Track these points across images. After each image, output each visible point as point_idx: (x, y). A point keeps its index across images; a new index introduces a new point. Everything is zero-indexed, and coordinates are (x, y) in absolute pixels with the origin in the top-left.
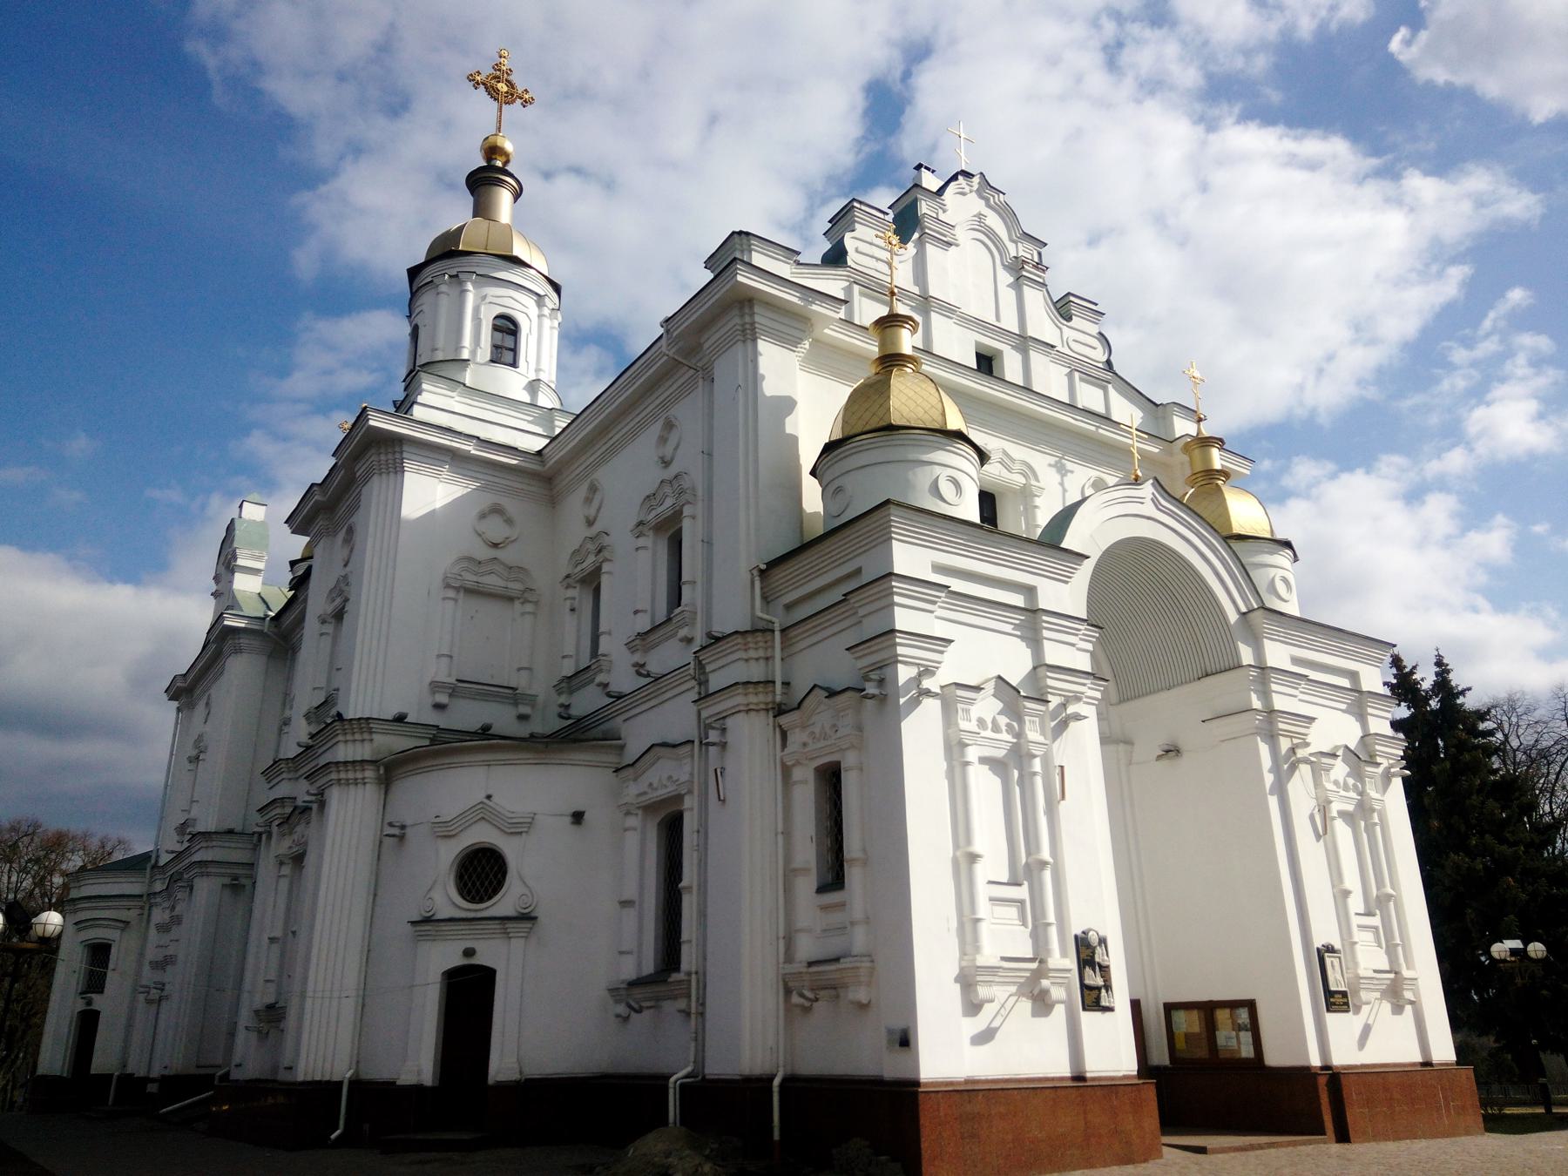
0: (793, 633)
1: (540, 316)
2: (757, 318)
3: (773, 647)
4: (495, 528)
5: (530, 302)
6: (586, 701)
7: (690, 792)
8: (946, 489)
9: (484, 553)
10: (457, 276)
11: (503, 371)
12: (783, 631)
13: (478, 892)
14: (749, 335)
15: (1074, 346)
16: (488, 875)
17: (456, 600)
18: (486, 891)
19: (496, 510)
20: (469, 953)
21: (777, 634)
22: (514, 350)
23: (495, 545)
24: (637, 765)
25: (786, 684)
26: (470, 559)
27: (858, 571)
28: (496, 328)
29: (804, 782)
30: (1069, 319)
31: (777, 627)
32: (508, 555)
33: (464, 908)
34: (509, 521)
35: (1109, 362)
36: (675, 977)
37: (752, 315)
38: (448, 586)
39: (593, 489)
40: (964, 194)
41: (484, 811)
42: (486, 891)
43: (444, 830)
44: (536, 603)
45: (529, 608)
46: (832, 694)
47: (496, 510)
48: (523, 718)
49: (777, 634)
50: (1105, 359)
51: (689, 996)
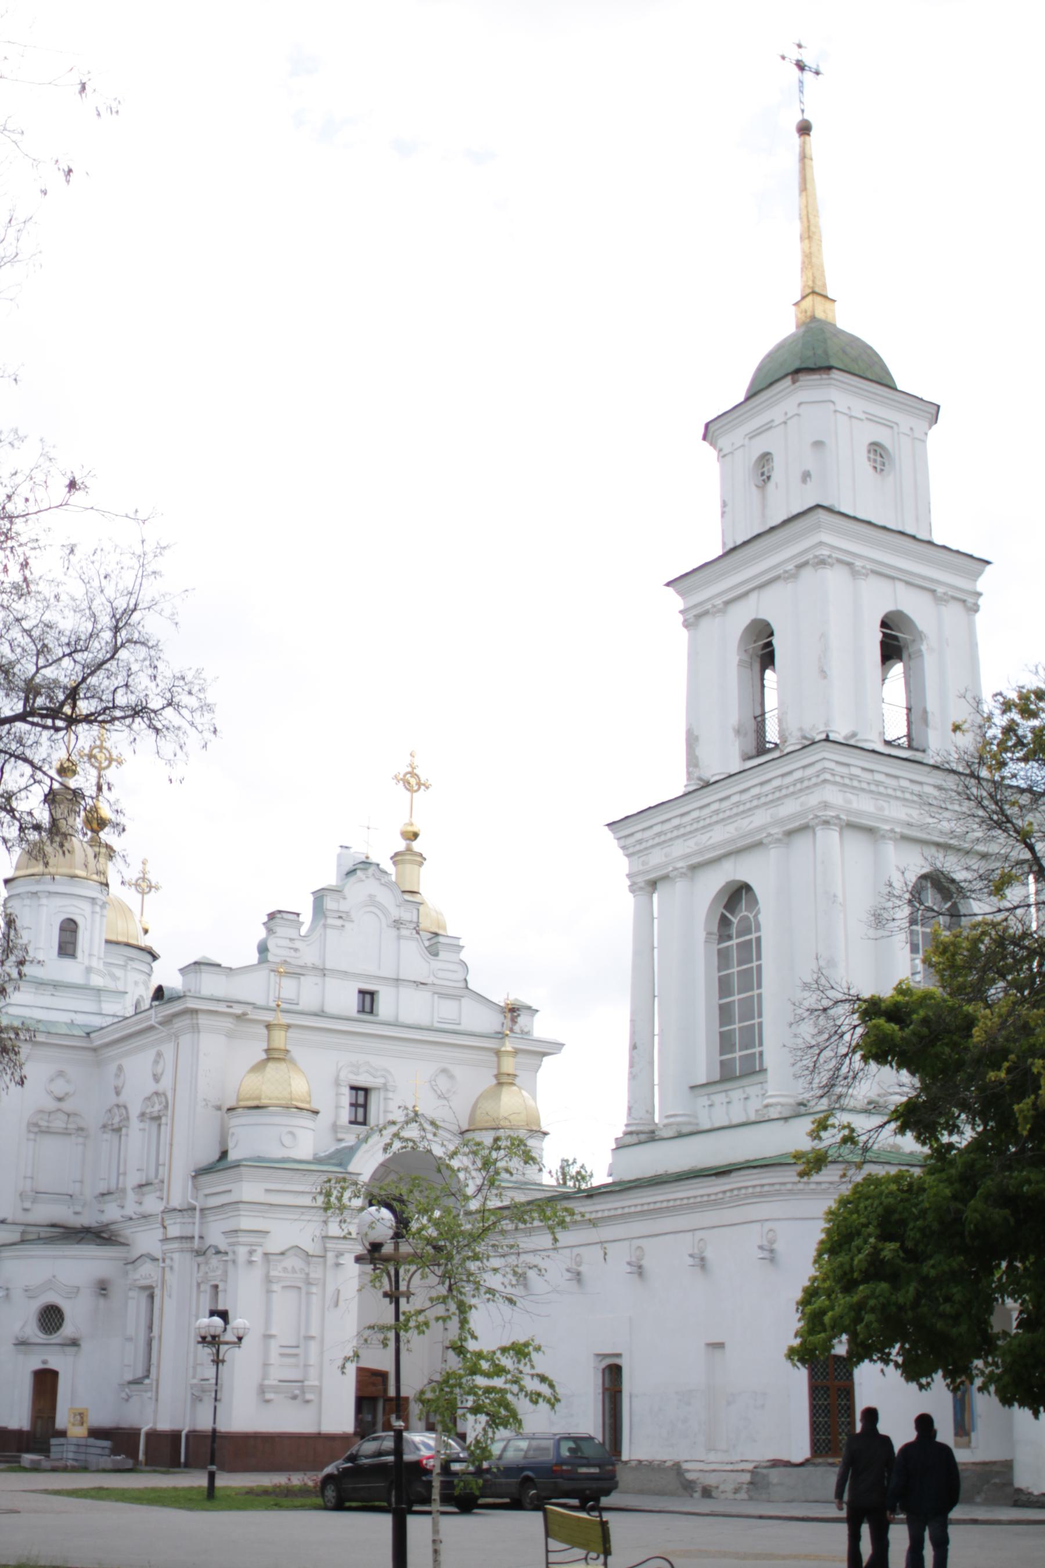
0: (207, 1212)
1: (93, 912)
2: (200, 1021)
3: (194, 1218)
4: (60, 1087)
5: (86, 906)
6: (111, 1213)
7: (157, 1286)
8: (287, 1140)
9: (51, 1104)
10: (36, 893)
11: (67, 962)
12: (202, 1210)
13: (49, 1328)
14: (196, 1029)
15: (441, 974)
16: (54, 1320)
17: (35, 1140)
18: (53, 1328)
19: (61, 1074)
20: (45, 1362)
21: (198, 1213)
22: (74, 943)
23: (60, 1099)
24: (136, 1263)
25: (201, 1237)
26: (41, 1111)
27: (230, 1191)
28: (62, 929)
29: (205, 1292)
30: (436, 955)
31: (198, 1209)
32: (66, 1106)
33: (39, 1337)
34: (68, 1081)
35: (465, 980)
36: (147, 1381)
37: (197, 1019)
38: (29, 1131)
39: (120, 1068)
40: (362, 881)
41: (50, 1284)
42: (53, 1328)
43: (29, 1293)
44: (86, 1137)
45: (80, 1140)
46: (218, 1252)
47: (61, 1074)
48: (76, 1213)
49: (198, 1213)
50: (463, 977)
51: (151, 1391)
